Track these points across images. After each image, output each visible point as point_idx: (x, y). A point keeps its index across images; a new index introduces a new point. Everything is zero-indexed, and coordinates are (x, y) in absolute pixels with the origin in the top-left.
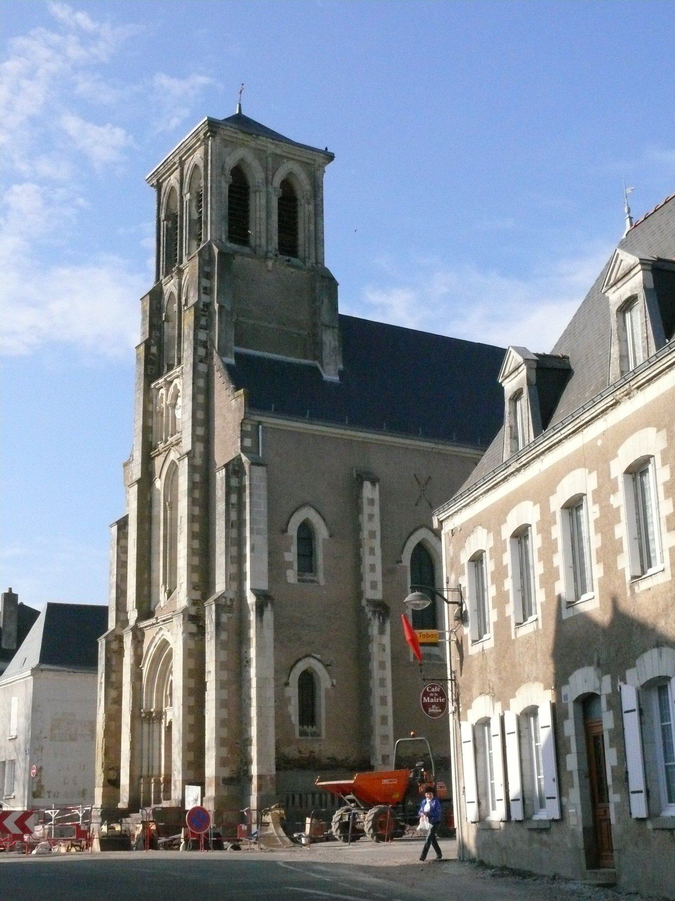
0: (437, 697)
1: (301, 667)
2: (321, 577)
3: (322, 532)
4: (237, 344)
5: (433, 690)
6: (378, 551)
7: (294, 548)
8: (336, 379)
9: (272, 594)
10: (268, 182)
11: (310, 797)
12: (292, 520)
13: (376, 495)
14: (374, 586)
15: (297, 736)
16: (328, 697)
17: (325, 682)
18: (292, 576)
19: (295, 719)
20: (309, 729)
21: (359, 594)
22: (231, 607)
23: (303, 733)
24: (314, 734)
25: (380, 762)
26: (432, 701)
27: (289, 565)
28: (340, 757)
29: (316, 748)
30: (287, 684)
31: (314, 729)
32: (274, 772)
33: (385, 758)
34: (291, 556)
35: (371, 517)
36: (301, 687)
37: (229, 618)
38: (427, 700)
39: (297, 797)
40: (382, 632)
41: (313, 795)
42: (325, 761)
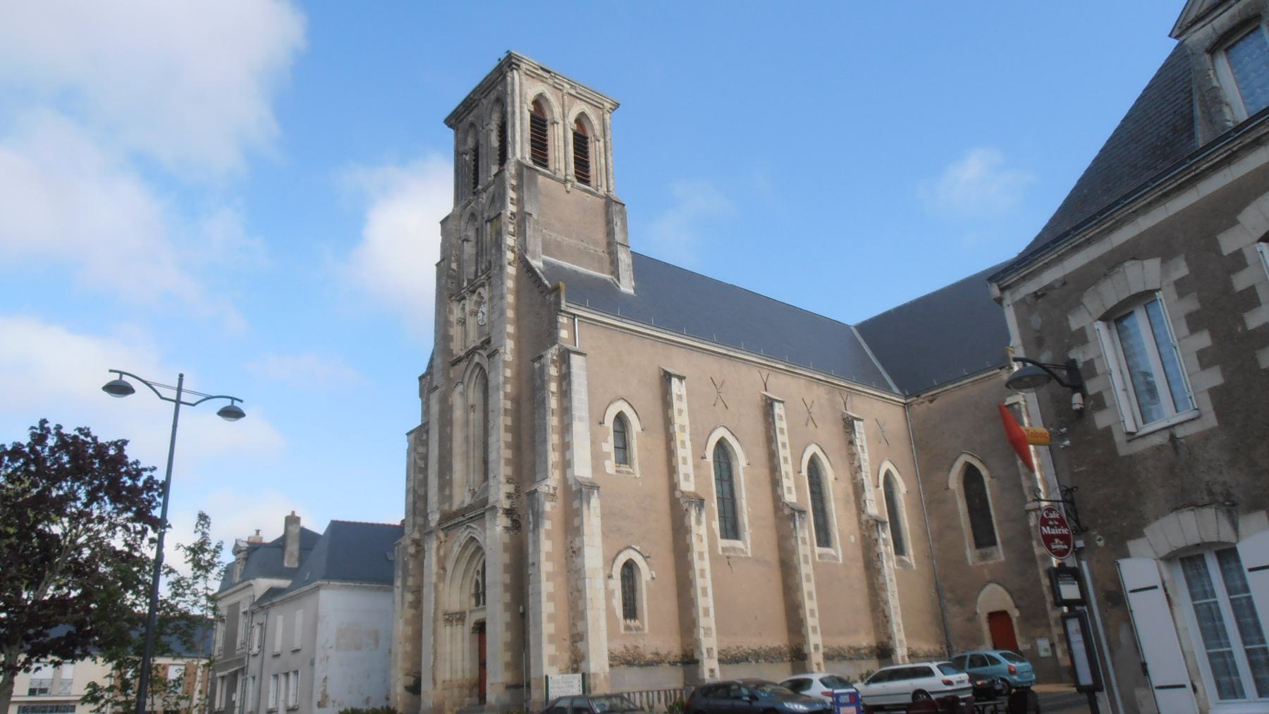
0: (1058, 527)
1: (622, 559)
2: (637, 470)
3: (635, 425)
4: (545, 252)
5: (1052, 516)
6: (688, 444)
7: (611, 438)
8: (632, 292)
9: (598, 482)
10: (564, 116)
11: (638, 695)
12: (611, 408)
13: (684, 392)
14: (687, 477)
15: (622, 631)
16: (648, 589)
17: (645, 574)
18: (610, 466)
19: (619, 612)
20: (632, 623)
21: (673, 486)
22: (553, 495)
23: (628, 628)
24: (637, 629)
25: (705, 655)
26: (1054, 532)
27: (607, 456)
28: (663, 652)
29: (641, 643)
30: (610, 577)
31: (638, 623)
32: (607, 668)
33: (709, 651)
34: (609, 446)
35: (680, 411)
36: (623, 577)
37: (553, 508)
38: (1047, 530)
39: (662, 694)
40: (699, 522)
41: (641, 693)
42: (649, 657)
